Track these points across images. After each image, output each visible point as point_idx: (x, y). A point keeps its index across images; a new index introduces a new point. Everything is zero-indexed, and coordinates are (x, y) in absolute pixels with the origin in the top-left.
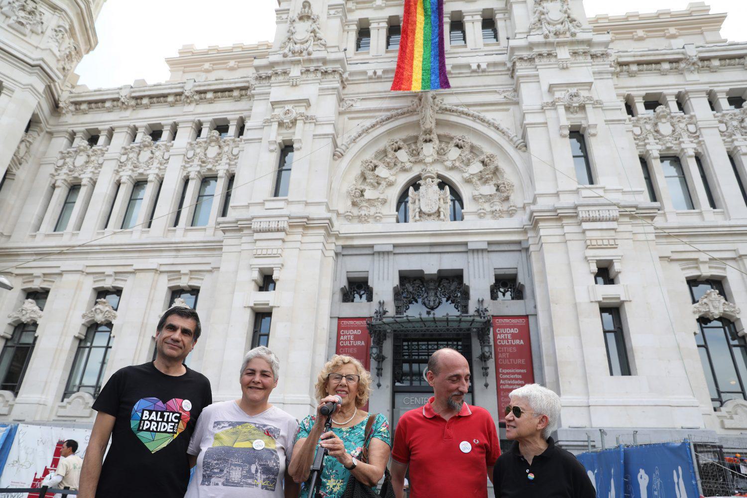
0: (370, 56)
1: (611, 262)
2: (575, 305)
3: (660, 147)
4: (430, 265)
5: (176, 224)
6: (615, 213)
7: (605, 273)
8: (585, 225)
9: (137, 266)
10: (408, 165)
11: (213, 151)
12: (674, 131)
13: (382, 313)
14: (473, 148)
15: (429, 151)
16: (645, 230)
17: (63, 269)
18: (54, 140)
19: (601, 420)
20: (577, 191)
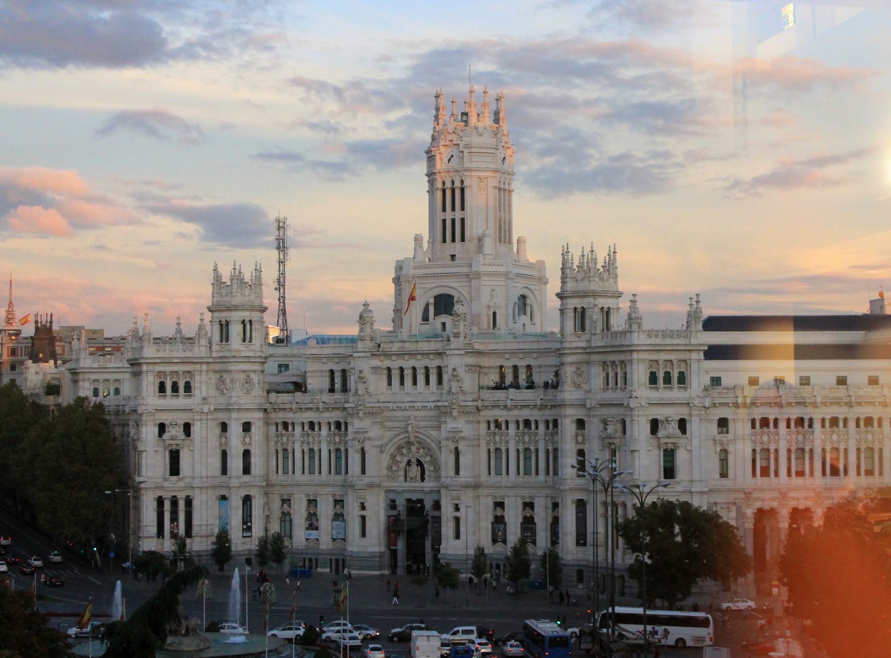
0: (390, 393)
1: (457, 505)
2: (447, 518)
3: (493, 448)
4: (414, 497)
5: (330, 473)
6: (459, 489)
7: (457, 509)
8: (452, 492)
9: (320, 493)
10: (407, 455)
11: (337, 439)
12: (500, 439)
13: (399, 515)
14: (428, 448)
15: (413, 449)
16: (470, 493)
17: (295, 492)
18: (269, 427)
19: (450, 552)
20: (451, 477)
